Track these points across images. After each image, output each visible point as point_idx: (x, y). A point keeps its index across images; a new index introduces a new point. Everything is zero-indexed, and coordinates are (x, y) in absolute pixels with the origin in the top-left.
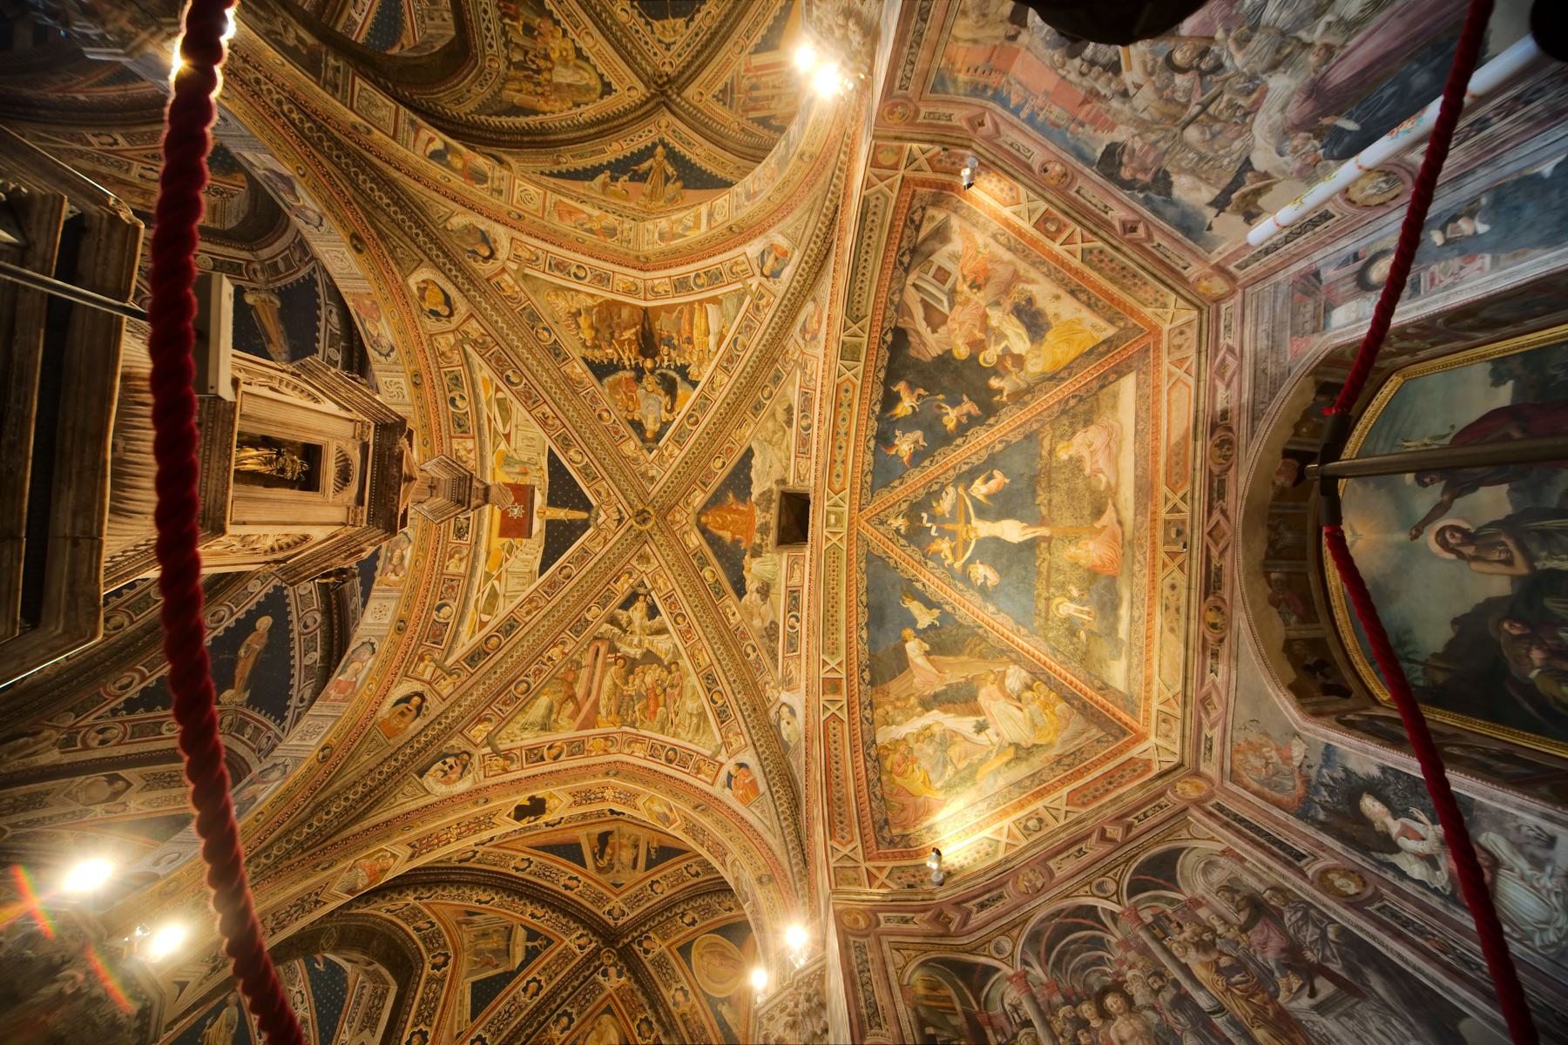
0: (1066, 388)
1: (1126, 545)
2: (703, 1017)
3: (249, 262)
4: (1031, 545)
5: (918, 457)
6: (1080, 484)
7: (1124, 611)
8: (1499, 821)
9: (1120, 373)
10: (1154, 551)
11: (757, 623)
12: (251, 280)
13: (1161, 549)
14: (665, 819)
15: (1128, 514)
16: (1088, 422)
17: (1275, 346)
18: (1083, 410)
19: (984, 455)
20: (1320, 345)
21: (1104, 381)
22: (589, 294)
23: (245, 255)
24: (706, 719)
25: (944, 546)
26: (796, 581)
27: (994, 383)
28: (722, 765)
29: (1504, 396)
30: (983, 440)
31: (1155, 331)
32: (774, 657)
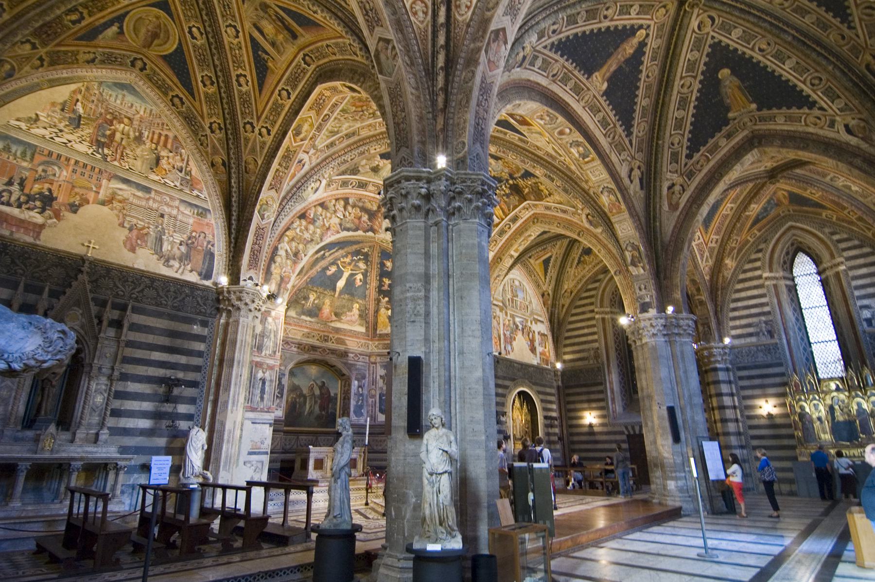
0: (371, 312)
1: (325, 323)
2: (109, 10)
3: (755, 124)
4: (334, 289)
5: (382, 265)
6: (345, 310)
7: (308, 319)
8: (281, 401)
9: (367, 328)
10: (324, 331)
11: (364, 162)
12: (753, 116)
13: (322, 334)
14: (297, 133)
15: (333, 324)
16: (360, 316)
17: (356, 369)
18: (363, 316)
19: (368, 282)
20: (354, 378)
21: (367, 322)
22: (549, 202)
23: (757, 127)
24: (333, 136)
25: (348, 260)
26: (371, 188)
27: (387, 299)
28: (308, 153)
29: (332, 395)
30: (373, 284)
31: (372, 340)
32: (343, 173)
